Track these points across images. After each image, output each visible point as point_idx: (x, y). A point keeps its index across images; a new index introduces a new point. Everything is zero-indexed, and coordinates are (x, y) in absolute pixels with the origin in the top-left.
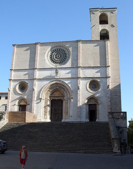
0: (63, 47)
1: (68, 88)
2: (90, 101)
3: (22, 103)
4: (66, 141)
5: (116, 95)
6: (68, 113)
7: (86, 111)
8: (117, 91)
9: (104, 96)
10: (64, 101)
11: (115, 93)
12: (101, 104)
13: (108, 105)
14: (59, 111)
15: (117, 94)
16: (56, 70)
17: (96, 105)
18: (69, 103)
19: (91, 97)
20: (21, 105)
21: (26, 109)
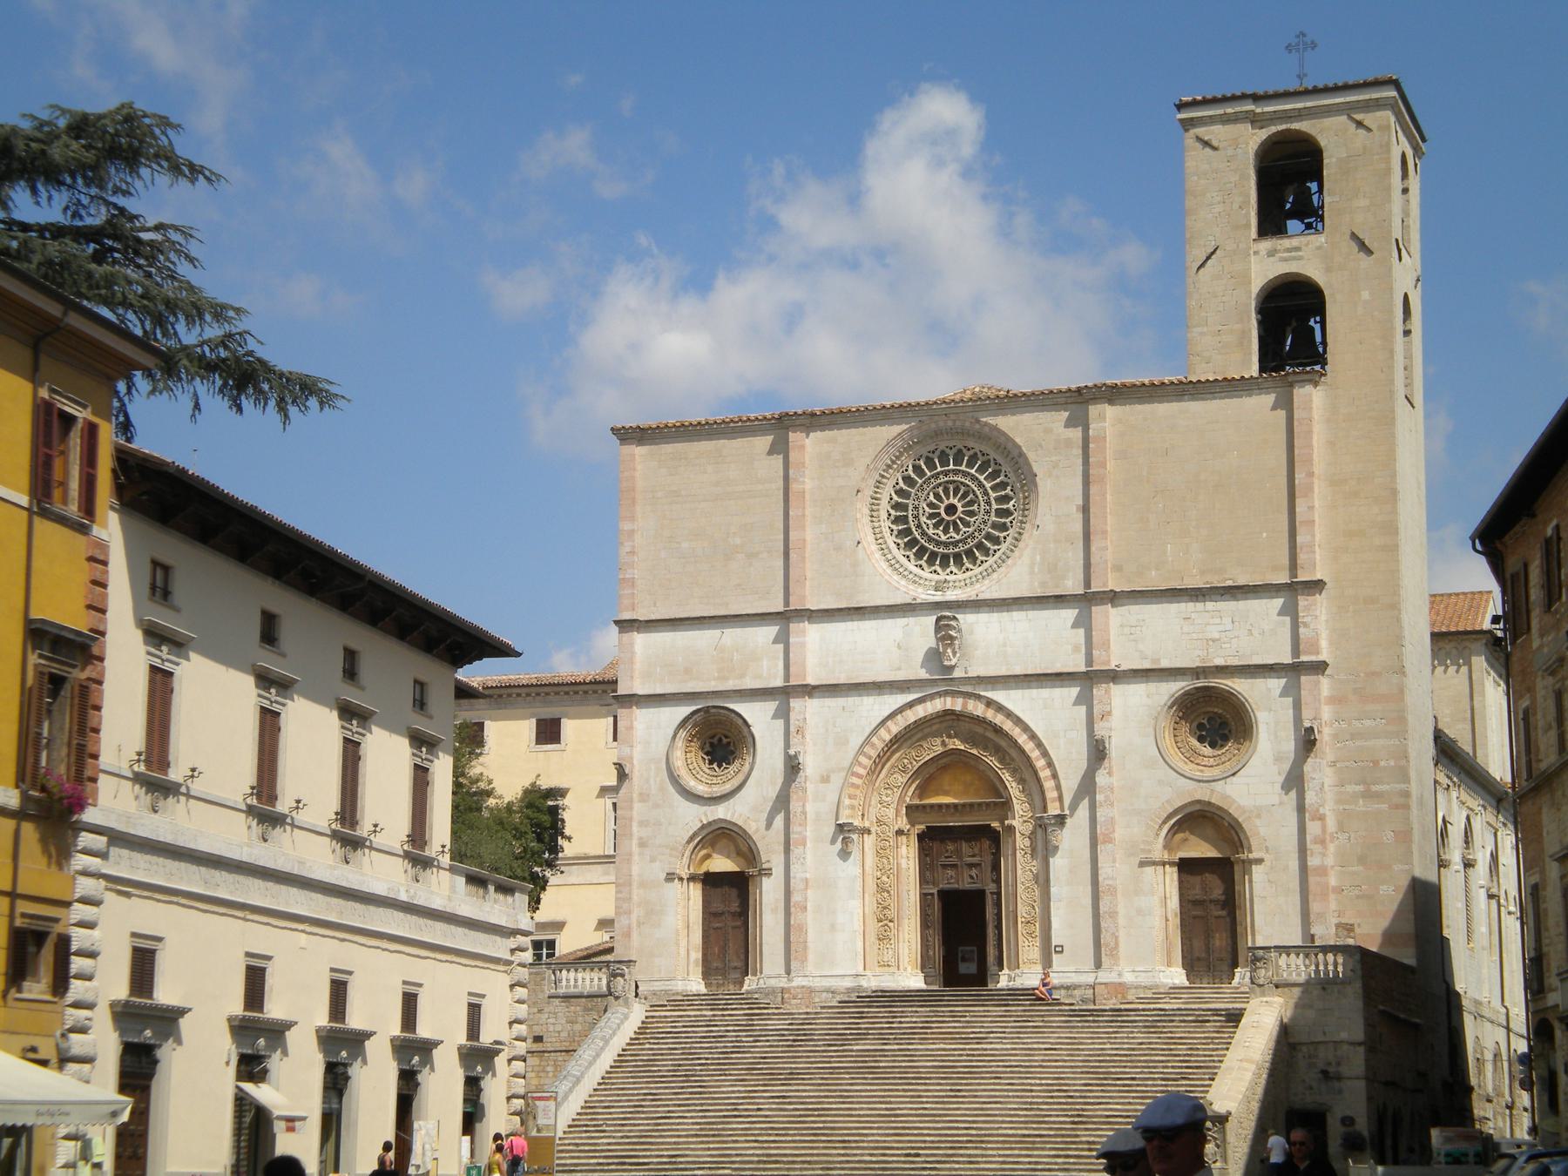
3: (722, 864)
5: (1368, 795)
8: (1376, 763)
11: (1364, 782)
15: (1374, 788)
16: (945, 615)
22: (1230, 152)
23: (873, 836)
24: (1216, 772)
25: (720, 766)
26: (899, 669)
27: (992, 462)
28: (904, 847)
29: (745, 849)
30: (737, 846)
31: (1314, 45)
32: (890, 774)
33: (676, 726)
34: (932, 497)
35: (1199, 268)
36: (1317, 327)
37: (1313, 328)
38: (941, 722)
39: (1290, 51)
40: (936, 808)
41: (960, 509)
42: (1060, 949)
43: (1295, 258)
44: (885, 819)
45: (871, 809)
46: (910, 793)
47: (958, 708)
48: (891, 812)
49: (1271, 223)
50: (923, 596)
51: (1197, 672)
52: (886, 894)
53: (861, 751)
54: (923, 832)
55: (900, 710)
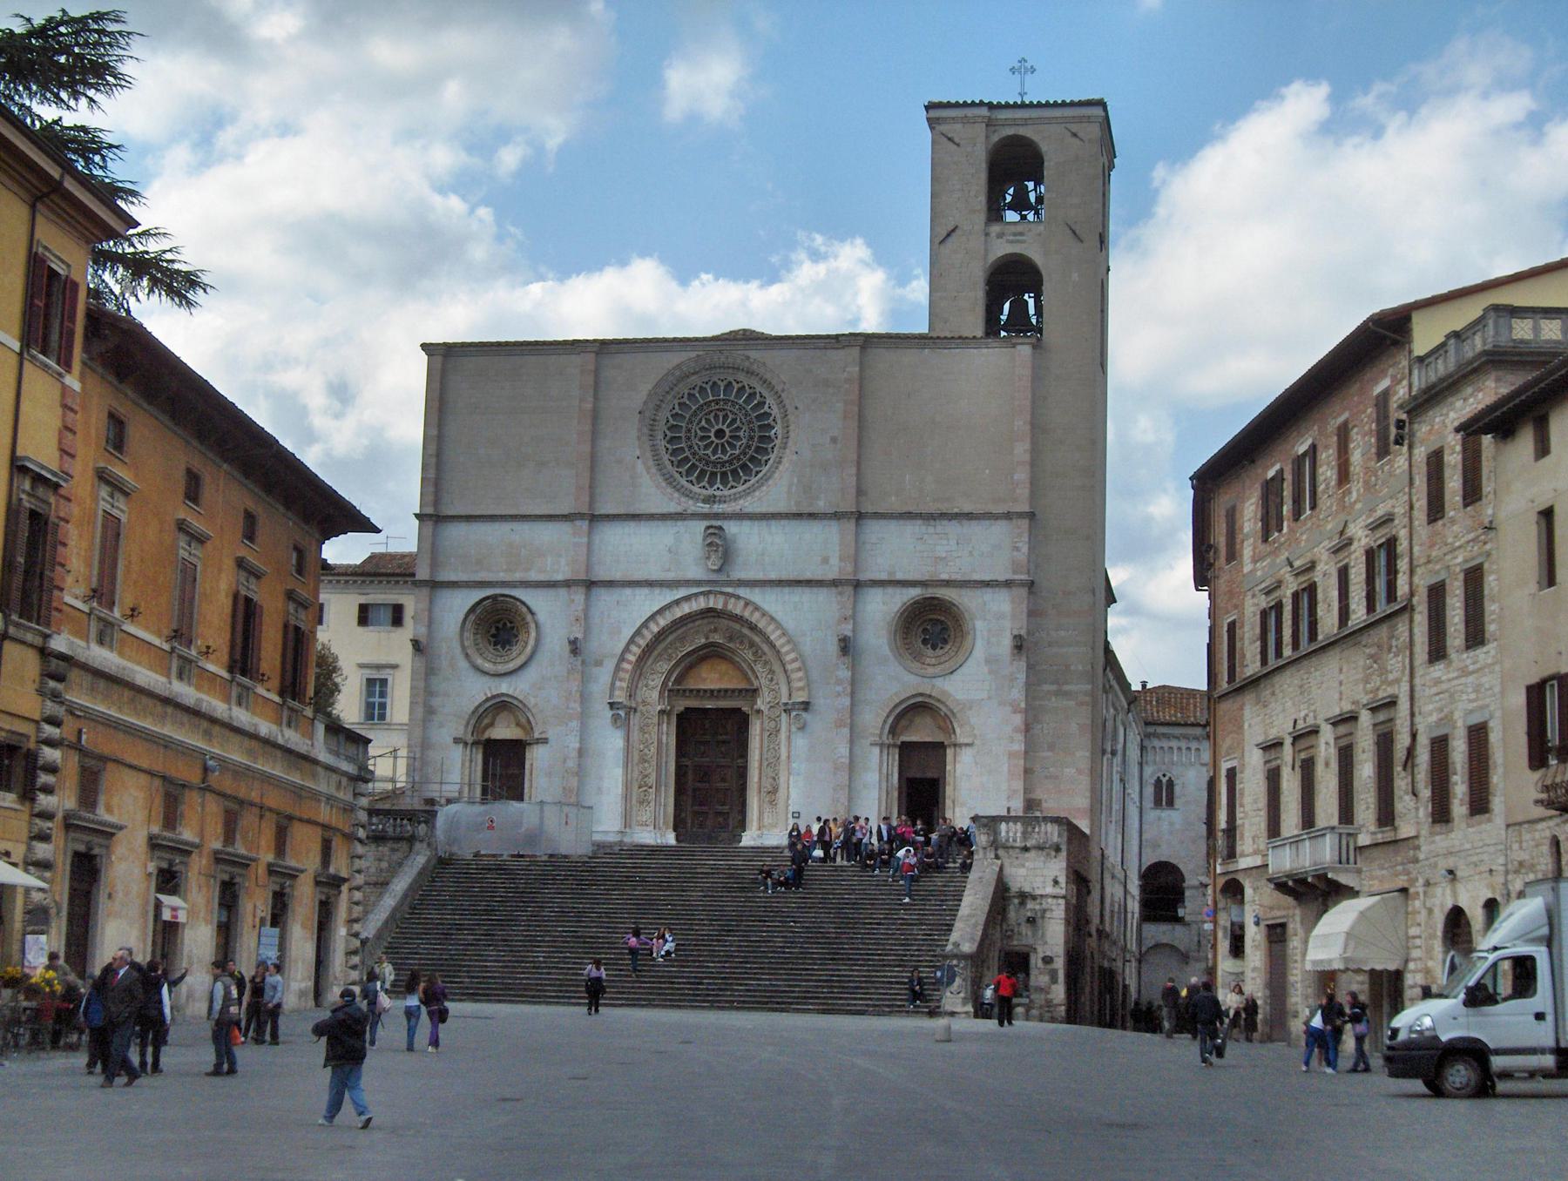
0: (750, 373)
1: (778, 644)
2: (906, 728)
3: (503, 731)
4: (751, 960)
5: (1059, 693)
6: (782, 793)
7: (884, 785)
9: (989, 698)
11: (1058, 684)
12: (967, 745)
13: (1011, 755)
15: (1067, 688)
17: (941, 747)
18: (783, 735)
19: (912, 701)
20: (495, 740)
21: (527, 766)
22: (969, 149)
23: (638, 714)
24: (937, 670)
25: (503, 648)
26: (669, 570)
27: (758, 395)
28: (665, 725)
29: (523, 721)
30: (516, 717)
31: (1033, 70)
32: (656, 661)
33: (466, 610)
34: (703, 423)
35: (941, 242)
36: (1031, 302)
37: (1027, 302)
38: (703, 618)
39: (1014, 73)
41: (728, 434)
42: (796, 815)
43: (1018, 241)
44: (649, 700)
45: (638, 691)
46: (673, 679)
47: (720, 606)
48: (655, 694)
49: (994, 212)
50: (693, 508)
51: (923, 584)
52: (646, 765)
53: (632, 641)
55: (668, 607)
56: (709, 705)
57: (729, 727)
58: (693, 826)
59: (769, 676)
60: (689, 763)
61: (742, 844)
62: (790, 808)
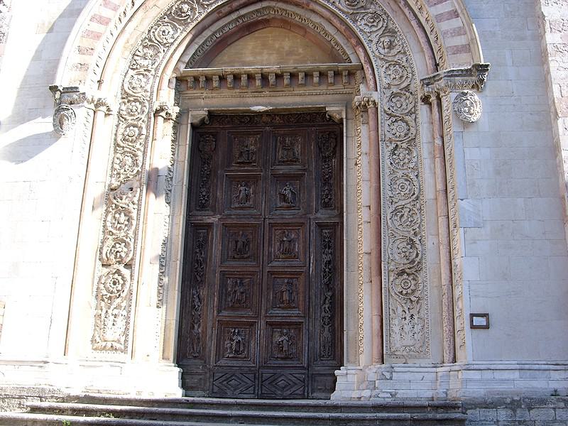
10: (364, 130)
14: (288, 253)
40: (230, 79)
54: (203, 121)
56: (259, 105)
57: (298, 149)
58: (219, 355)
59: (387, 39)
60: (214, 219)
61: (337, 397)
62: (459, 305)
